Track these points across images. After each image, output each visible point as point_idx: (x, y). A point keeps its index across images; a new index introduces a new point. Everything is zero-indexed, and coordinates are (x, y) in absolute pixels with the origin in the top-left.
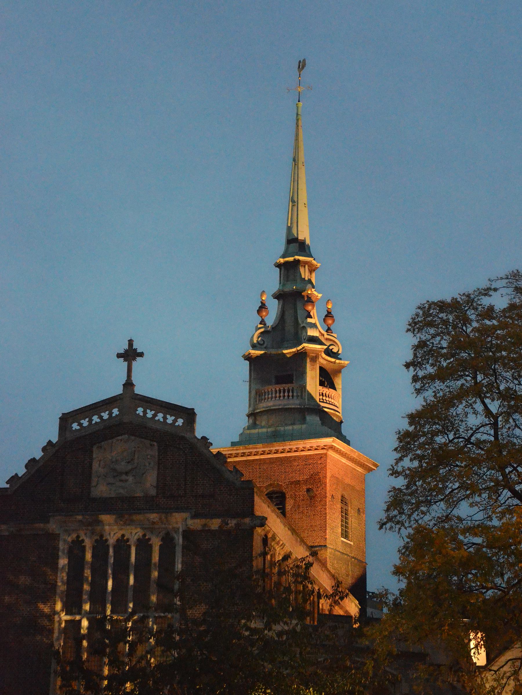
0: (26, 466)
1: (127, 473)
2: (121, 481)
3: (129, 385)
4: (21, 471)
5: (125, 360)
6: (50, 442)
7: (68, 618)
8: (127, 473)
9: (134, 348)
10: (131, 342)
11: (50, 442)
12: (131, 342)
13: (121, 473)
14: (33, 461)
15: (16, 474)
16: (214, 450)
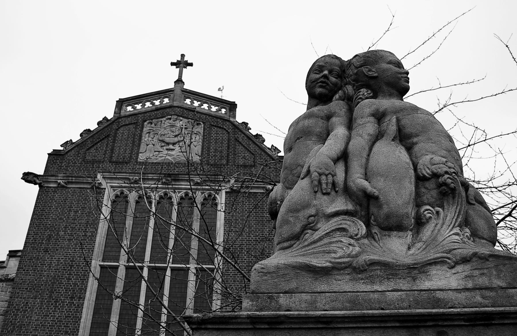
0: (81, 135)
1: (174, 144)
3: (179, 81)
4: (76, 138)
8: (174, 144)
9: (185, 60)
10: (183, 56)
11: (105, 118)
12: (183, 56)
13: (168, 144)
14: (88, 131)
15: (71, 140)
16: (253, 132)
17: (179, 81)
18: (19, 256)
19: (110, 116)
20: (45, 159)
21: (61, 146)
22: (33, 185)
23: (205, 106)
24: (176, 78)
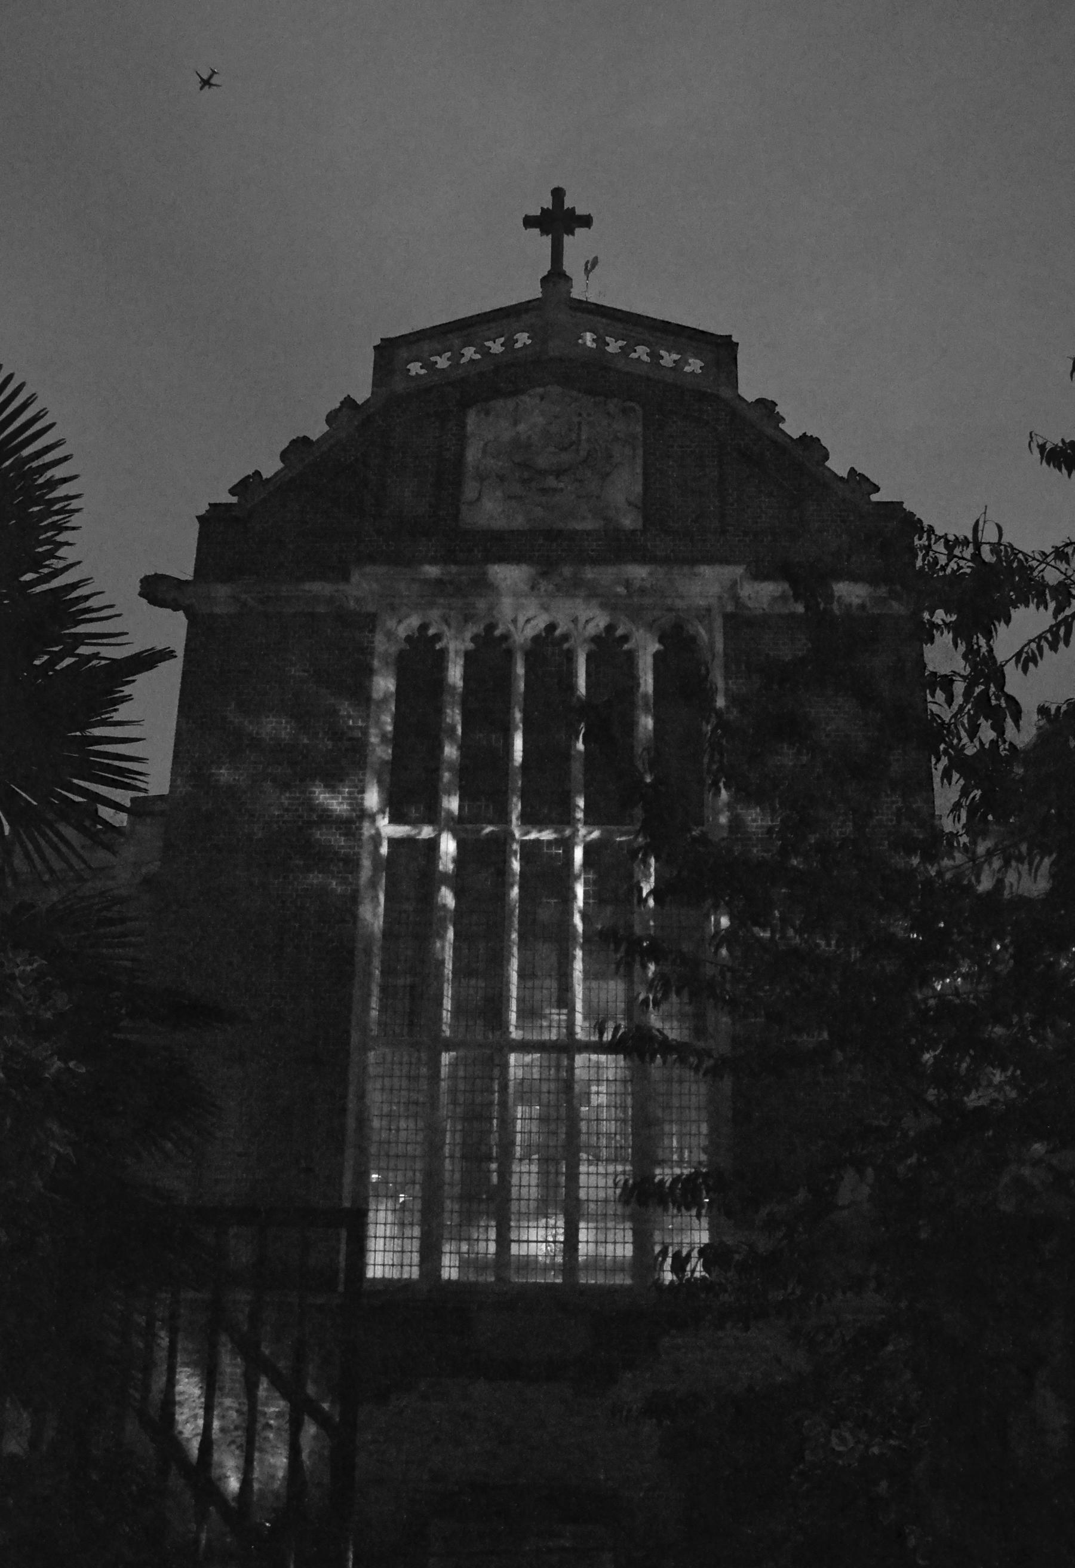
1: (559, 474)
2: (544, 491)
3: (556, 277)
5: (544, 232)
6: (349, 402)
7: (400, 831)
9: (565, 208)
10: (558, 194)
11: (349, 402)
12: (558, 194)
13: (543, 473)
14: (301, 443)
15: (257, 473)
16: (792, 428)
17: (556, 277)
18: (162, 813)
19: (362, 394)
20: (194, 530)
21: (233, 491)
22: (169, 611)
23: (641, 352)
24: (546, 267)
